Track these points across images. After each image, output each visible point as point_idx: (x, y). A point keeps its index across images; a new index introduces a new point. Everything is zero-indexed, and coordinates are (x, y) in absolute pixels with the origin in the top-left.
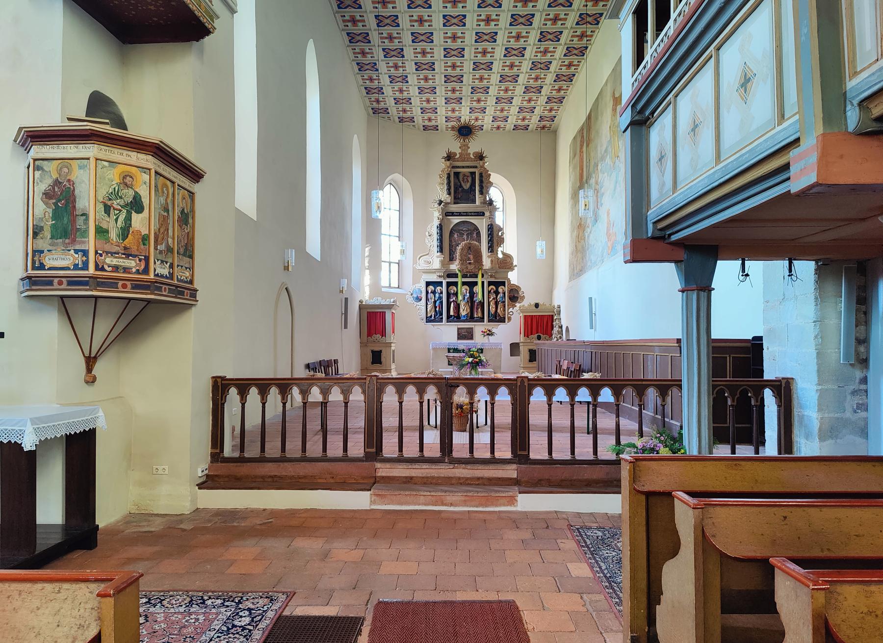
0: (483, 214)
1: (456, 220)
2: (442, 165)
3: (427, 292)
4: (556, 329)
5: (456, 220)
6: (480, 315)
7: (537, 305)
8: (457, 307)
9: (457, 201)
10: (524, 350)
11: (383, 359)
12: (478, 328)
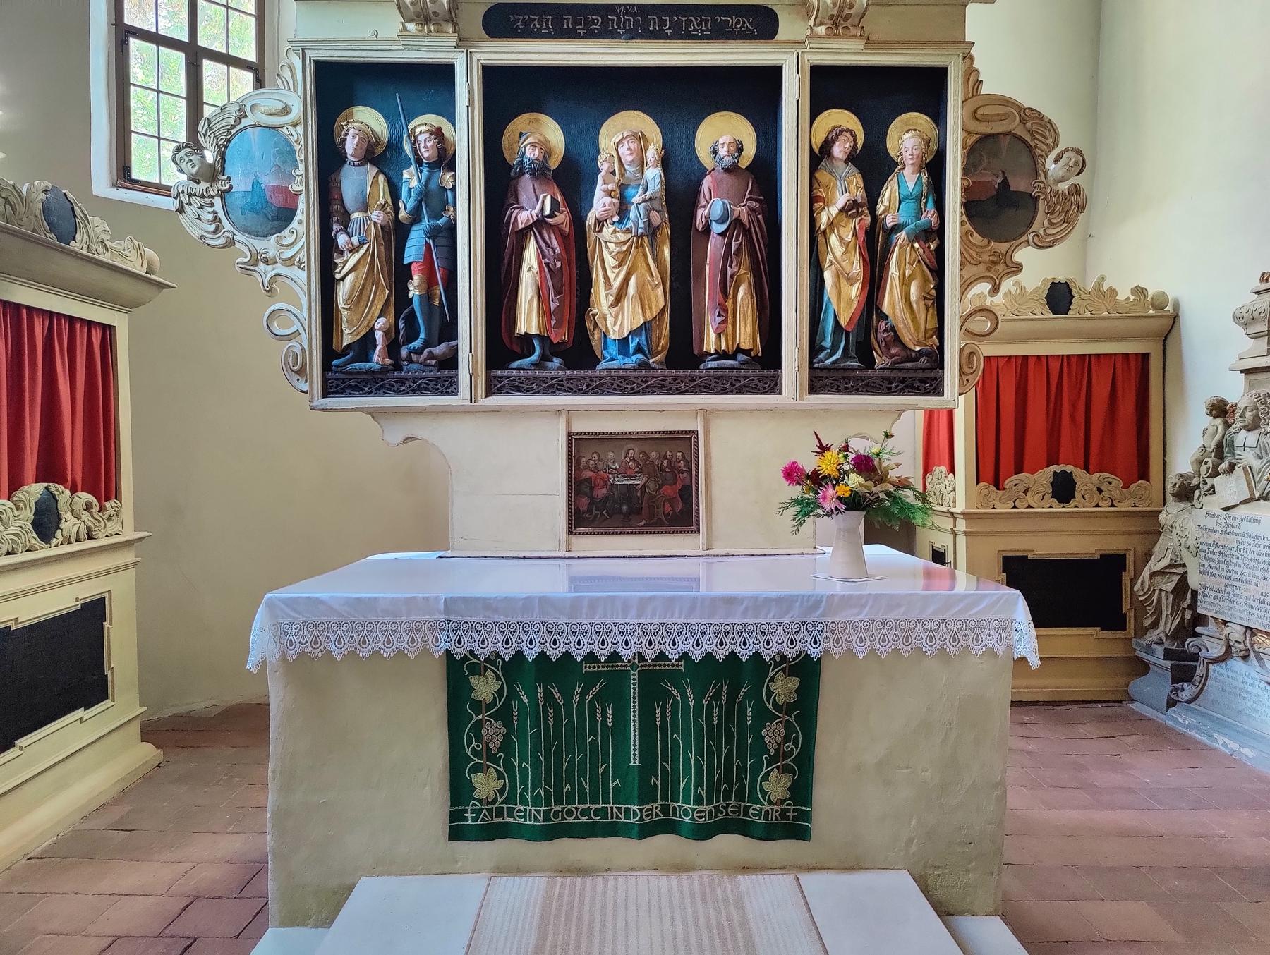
3: (330, 159)
6: (745, 334)
8: (573, 277)
12: (749, 445)
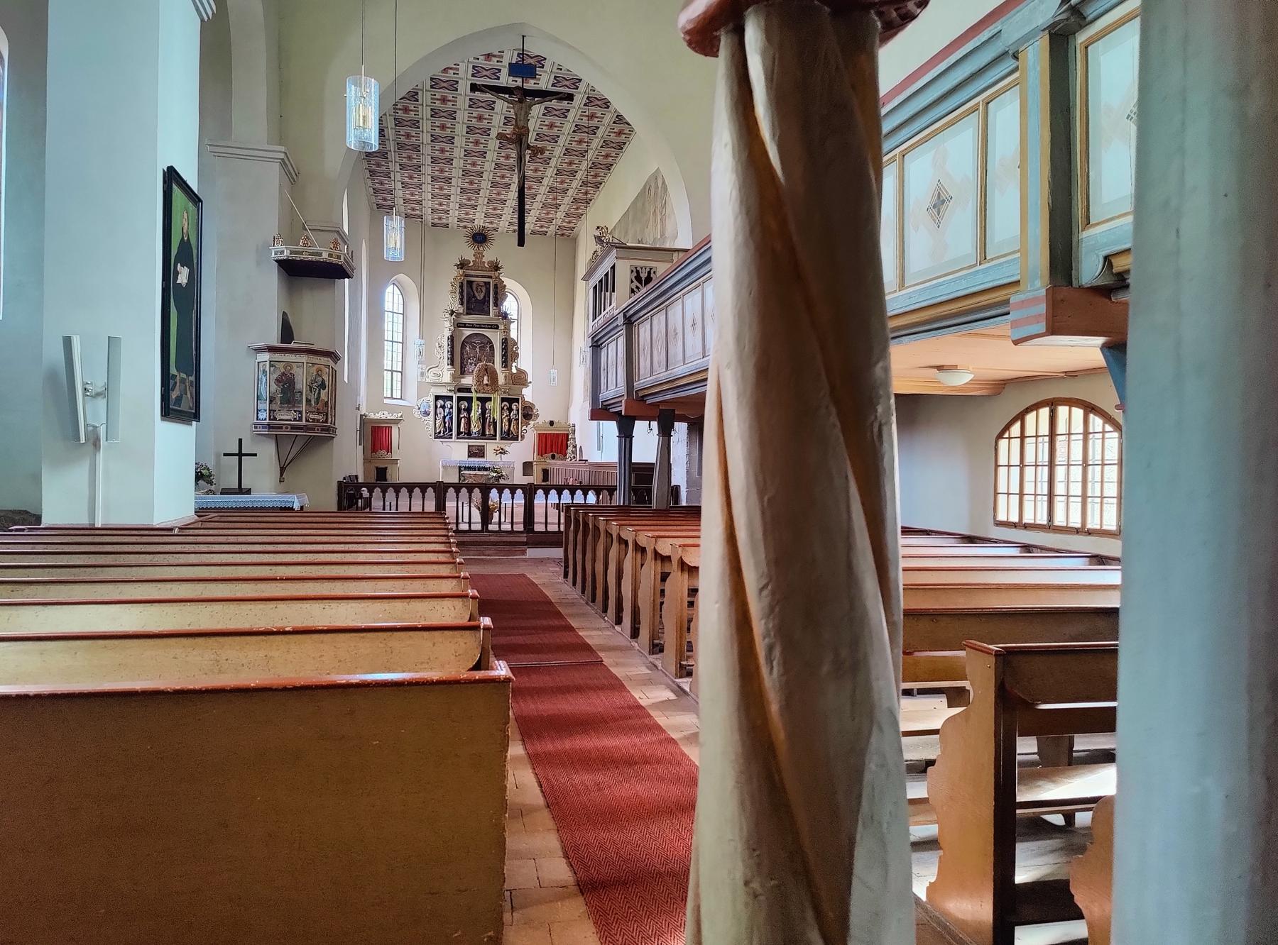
0: (497, 327)
1: (468, 332)
2: (455, 272)
4: (570, 449)
5: (468, 332)
7: (552, 423)
9: (469, 311)
10: (537, 470)
11: (388, 476)
12: (490, 446)
